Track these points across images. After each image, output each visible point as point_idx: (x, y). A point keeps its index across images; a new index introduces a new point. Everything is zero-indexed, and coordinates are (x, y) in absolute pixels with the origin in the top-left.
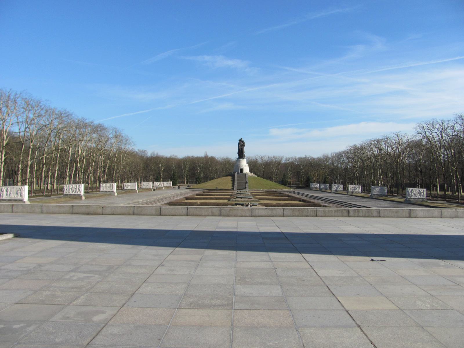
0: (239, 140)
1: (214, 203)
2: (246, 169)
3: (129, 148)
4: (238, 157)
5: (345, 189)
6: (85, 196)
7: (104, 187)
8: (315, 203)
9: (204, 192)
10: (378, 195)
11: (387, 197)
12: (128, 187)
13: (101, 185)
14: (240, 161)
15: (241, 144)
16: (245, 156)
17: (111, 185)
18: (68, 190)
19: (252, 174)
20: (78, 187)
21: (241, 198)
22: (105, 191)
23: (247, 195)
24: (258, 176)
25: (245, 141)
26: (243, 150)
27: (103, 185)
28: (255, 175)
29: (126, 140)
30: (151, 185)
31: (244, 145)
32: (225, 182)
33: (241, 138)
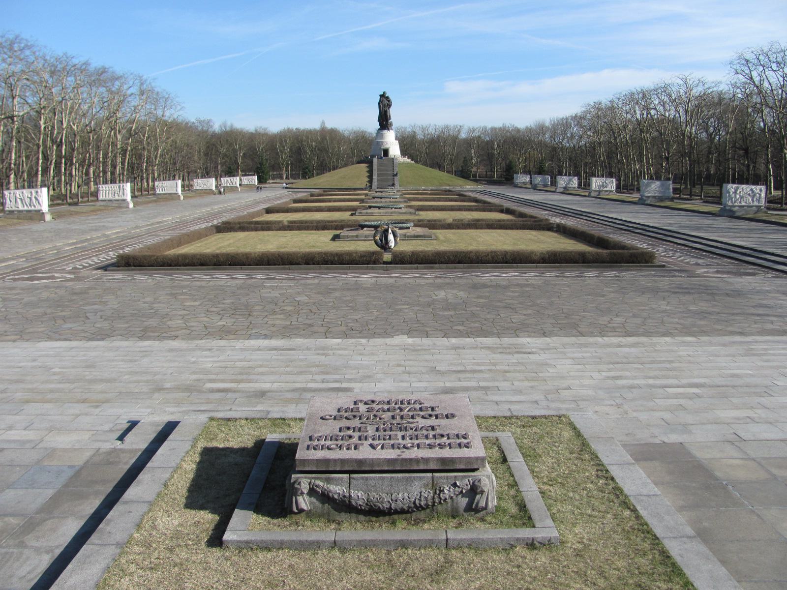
0: (380, 95)
1: (319, 222)
2: (395, 150)
3: (170, 115)
4: (379, 127)
5: (585, 185)
6: (52, 214)
7: (106, 191)
8: (535, 217)
9: (312, 195)
10: (654, 197)
11: (673, 201)
12: (162, 190)
13: (101, 188)
14: (382, 135)
15: (385, 103)
16: (391, 124)
17: (119, 187)
18: (13, 201)
19: (406, 158)
20: (34, 194)
21: (379, 208)
22: (109, 200)
23: (394, 200)
24: (417, 162)
25: (391, 97)
26: (388, 114)
27: (104, 188)
28: (412, 160)
29: (166, 100)
30: (211, 185)
31: (389, 106)
32: (356, 175)
33: (384, 92)
